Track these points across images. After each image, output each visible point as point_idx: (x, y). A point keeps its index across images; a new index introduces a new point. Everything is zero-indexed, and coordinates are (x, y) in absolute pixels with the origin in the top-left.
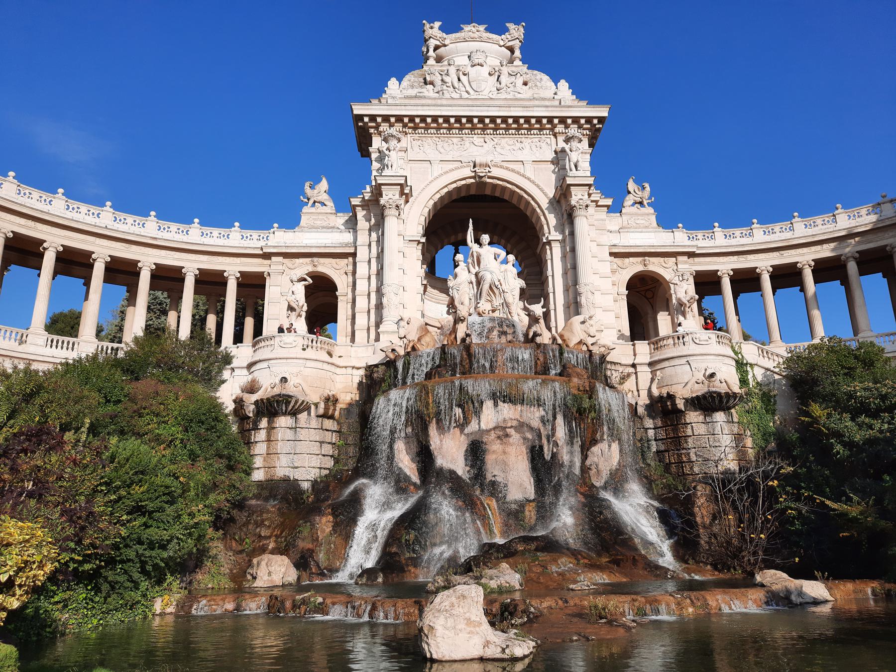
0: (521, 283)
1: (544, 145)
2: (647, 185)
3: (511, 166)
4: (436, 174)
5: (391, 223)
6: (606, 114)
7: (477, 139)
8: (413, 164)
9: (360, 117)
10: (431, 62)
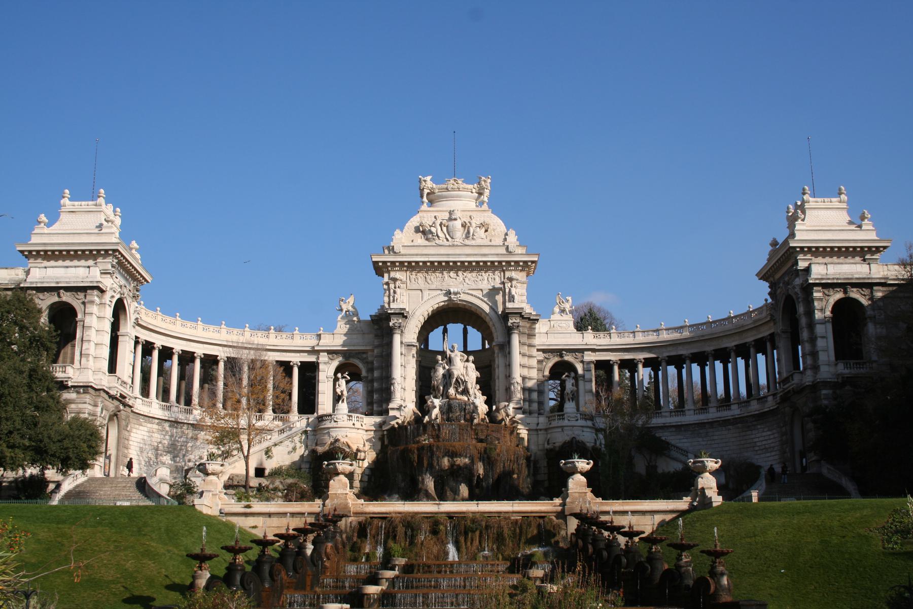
0: (478, 374)
2: (569, 298)
5: (397, 339)
6: (536, 259)
7: (452, 274)
8: (410, 292)
9: (375, 263)
10: (425, 207)
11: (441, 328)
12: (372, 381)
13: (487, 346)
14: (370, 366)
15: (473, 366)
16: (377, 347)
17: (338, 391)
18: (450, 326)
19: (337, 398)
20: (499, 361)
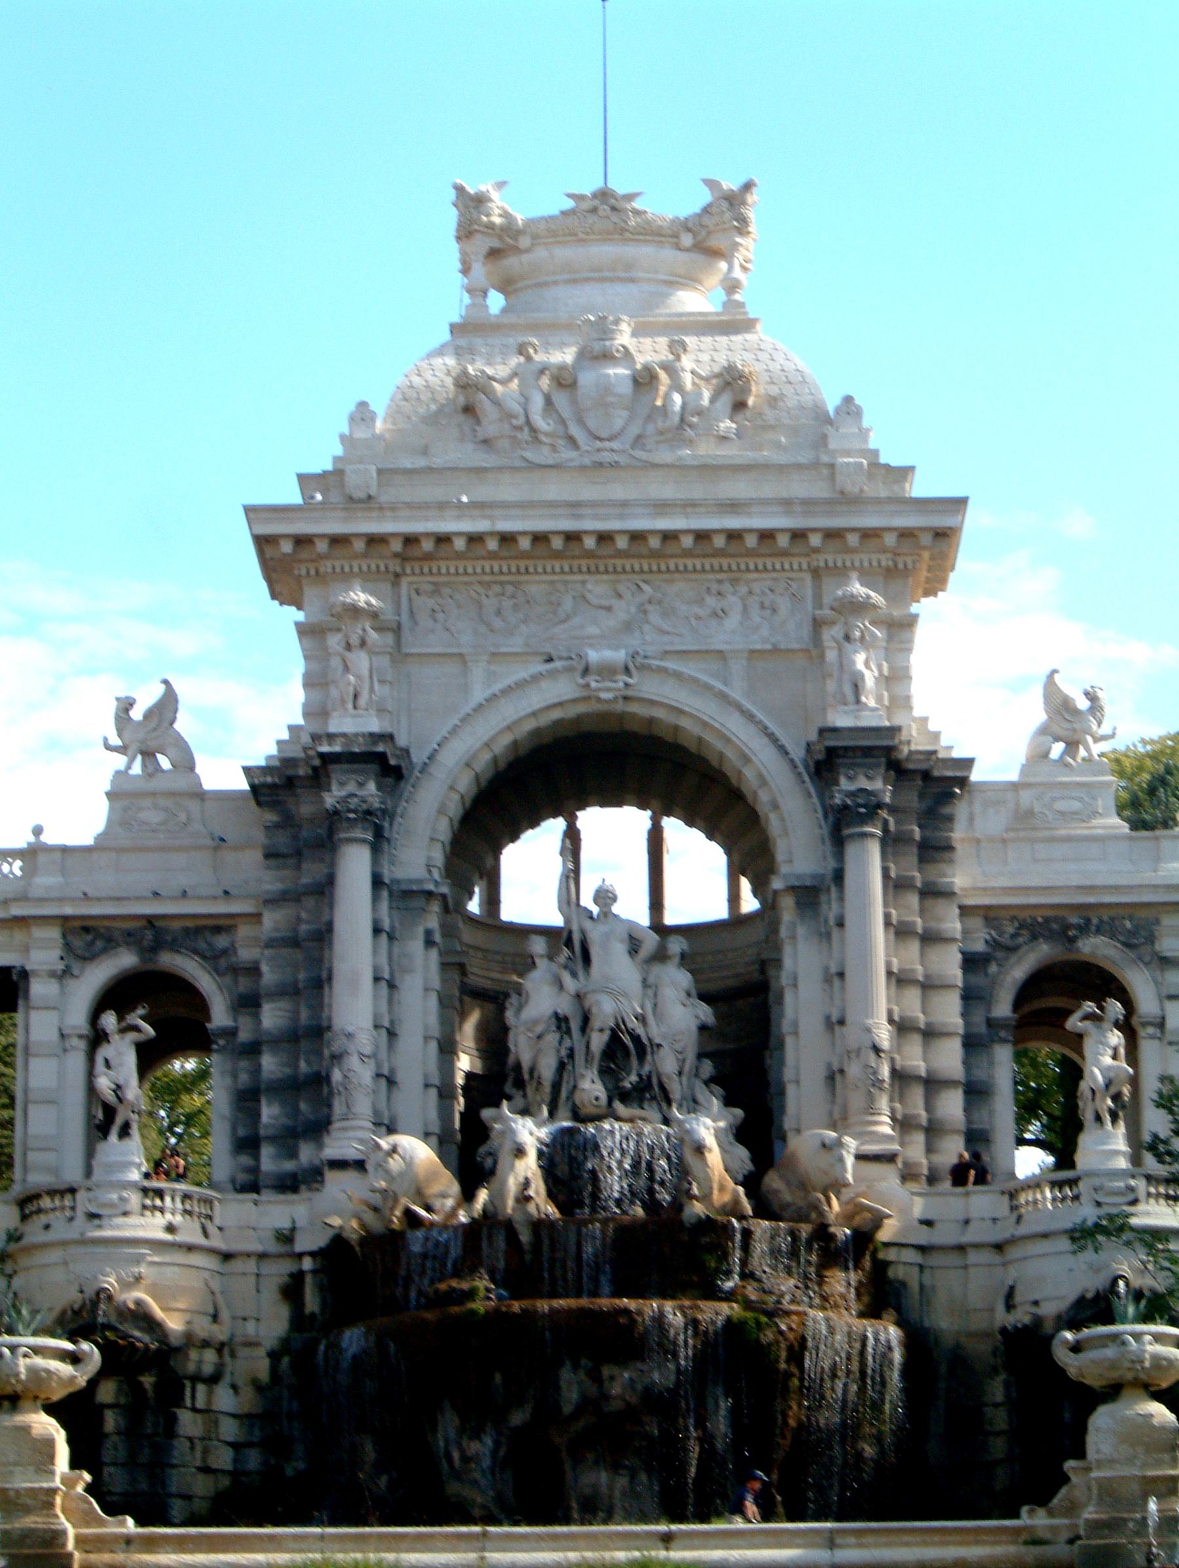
0: (705, 1013)
1: (784, 605)
3: (689, 668)
4: (479, 694)
5: (355, 865)
11: (555, 826)
12: (253, 1049)
13: (749, 903)
14: (244, 985)
15: (684, 979)
16: (273, 901)
17: (104, 1083)
18: (591, 819)
19: (104, 1120)
20: (800, 960)
